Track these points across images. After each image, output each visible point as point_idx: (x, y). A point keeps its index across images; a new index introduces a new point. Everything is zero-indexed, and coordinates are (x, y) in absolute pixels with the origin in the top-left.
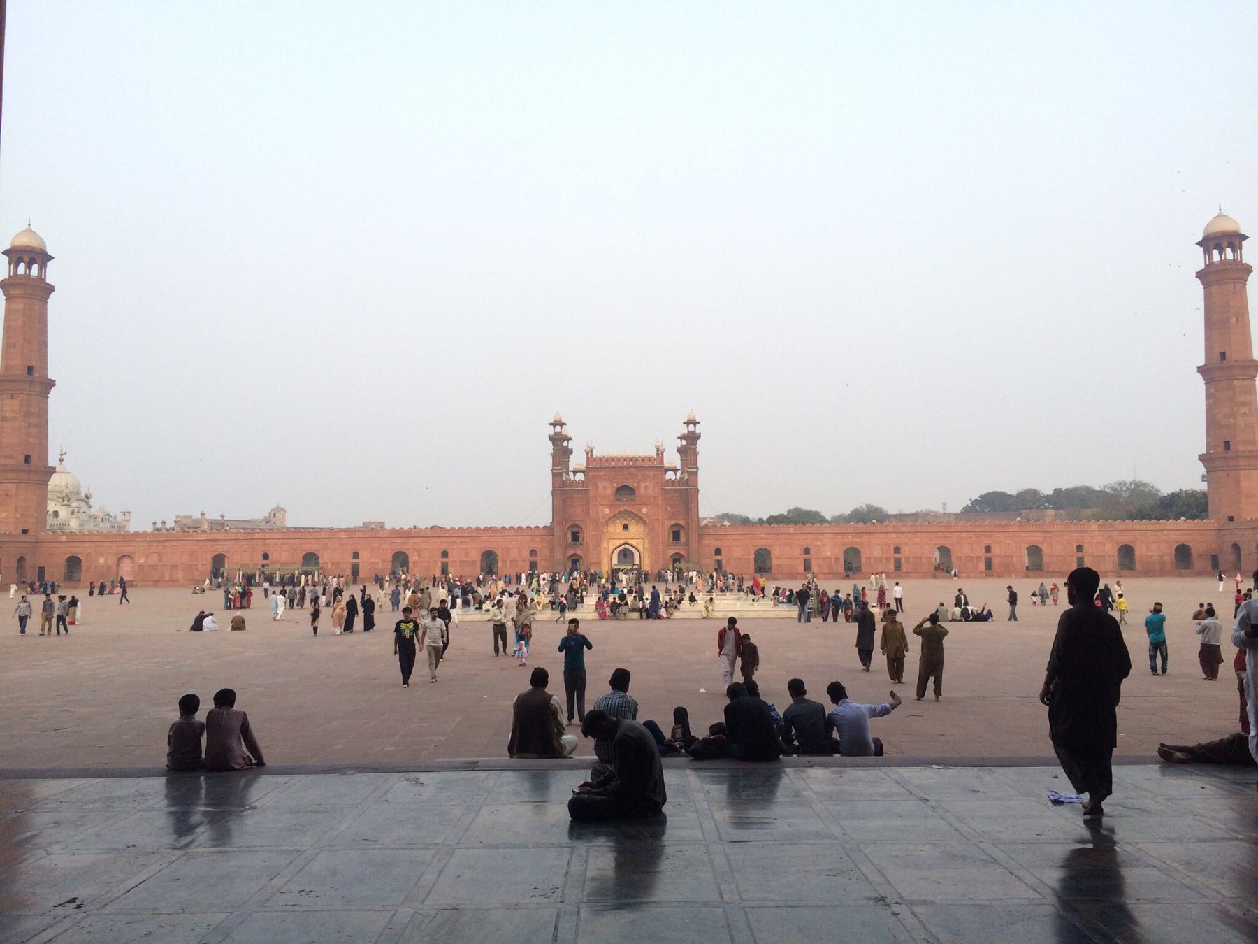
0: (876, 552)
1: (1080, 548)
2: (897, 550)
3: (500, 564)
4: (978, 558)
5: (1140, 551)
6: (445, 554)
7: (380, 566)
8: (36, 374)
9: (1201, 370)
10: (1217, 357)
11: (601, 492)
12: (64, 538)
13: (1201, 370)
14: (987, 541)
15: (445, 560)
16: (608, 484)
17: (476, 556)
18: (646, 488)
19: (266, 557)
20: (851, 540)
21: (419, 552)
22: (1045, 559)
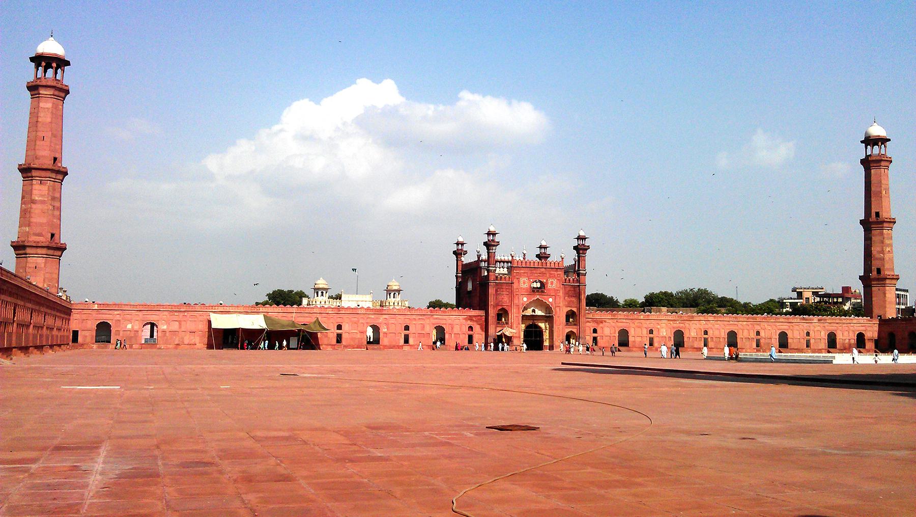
0: (693, 334)
1: (808, 334)
2: (706, 333)
5: (840, 337)
6: (407, 328)
7: (359, 336)
9: (862, 222)
10: (873, 215)
12: (96, 307)
14: (758, 328)
15: (407, 332)
16: (525, 279)
18: (552, 283)
20: (678, 325)
22: (790, 341)
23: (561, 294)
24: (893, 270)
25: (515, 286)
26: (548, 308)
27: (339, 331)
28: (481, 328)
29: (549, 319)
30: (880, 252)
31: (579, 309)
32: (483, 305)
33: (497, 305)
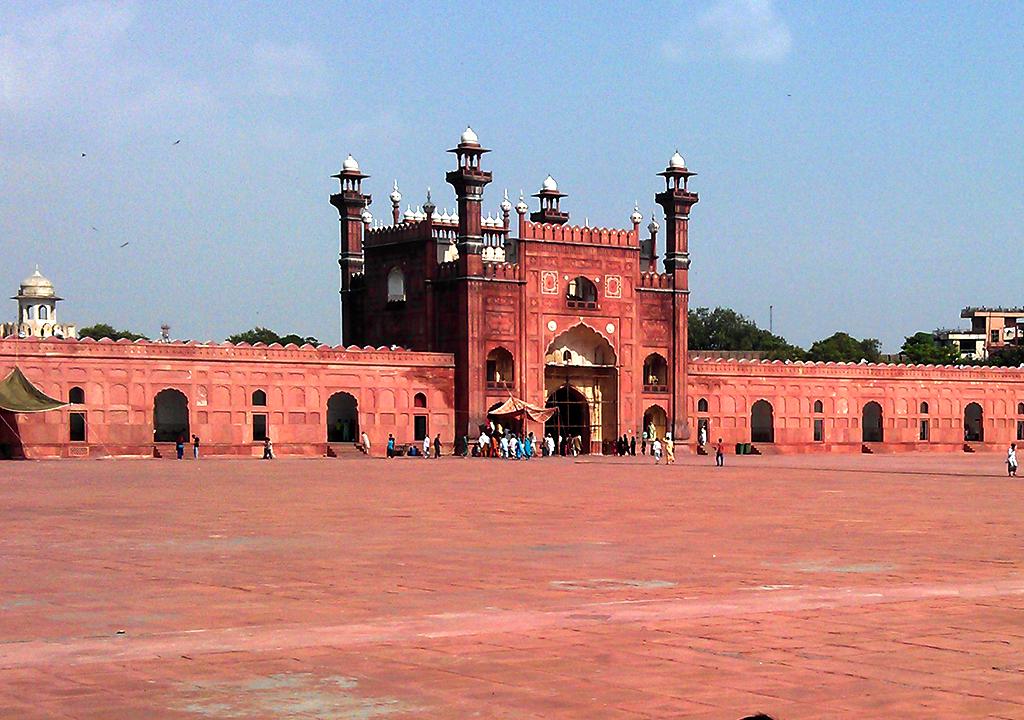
0: (901, 411)
2: (925, 408)
3: (362, 420)
7: (132, 419)
11: (545, 290)
16: (553, 274)
17: (318, 403)
18: (613, 286)
20: (872, 391)
21: (207, 389)
23: (634, 315)
25: (529, 290)
26: (601, 349)
27: (77, 408)
28: (448, 401)
29: (605, 375)
31: (673, 351)
32: (447, 335)
33: (485, 340)
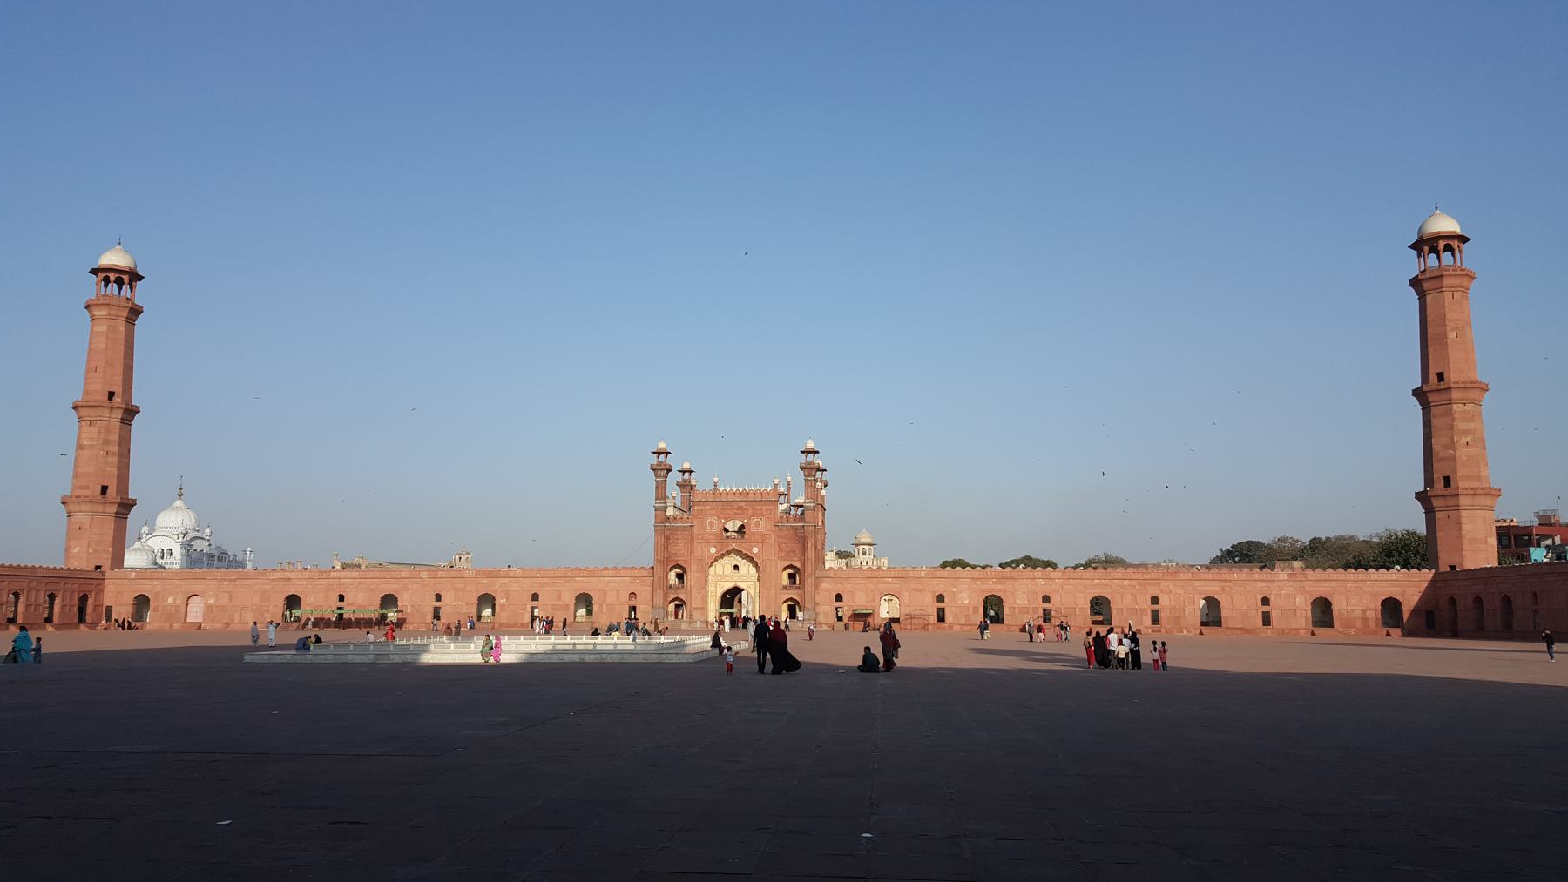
0: (1021, 601)
1: (1266, 601)
2: (1046, 599)
4: (1143, 611)
8: (117, 399)
9: (1417, 393)
10: (1433, 378)
13: (1417, 393)
16: (715, 519)
18: (758, 524)
19: (341, 598)
20: (992, 587)
21: (507, 594)
24: (1478, 478)
25: (696, 530)
30: (1445, 447)
